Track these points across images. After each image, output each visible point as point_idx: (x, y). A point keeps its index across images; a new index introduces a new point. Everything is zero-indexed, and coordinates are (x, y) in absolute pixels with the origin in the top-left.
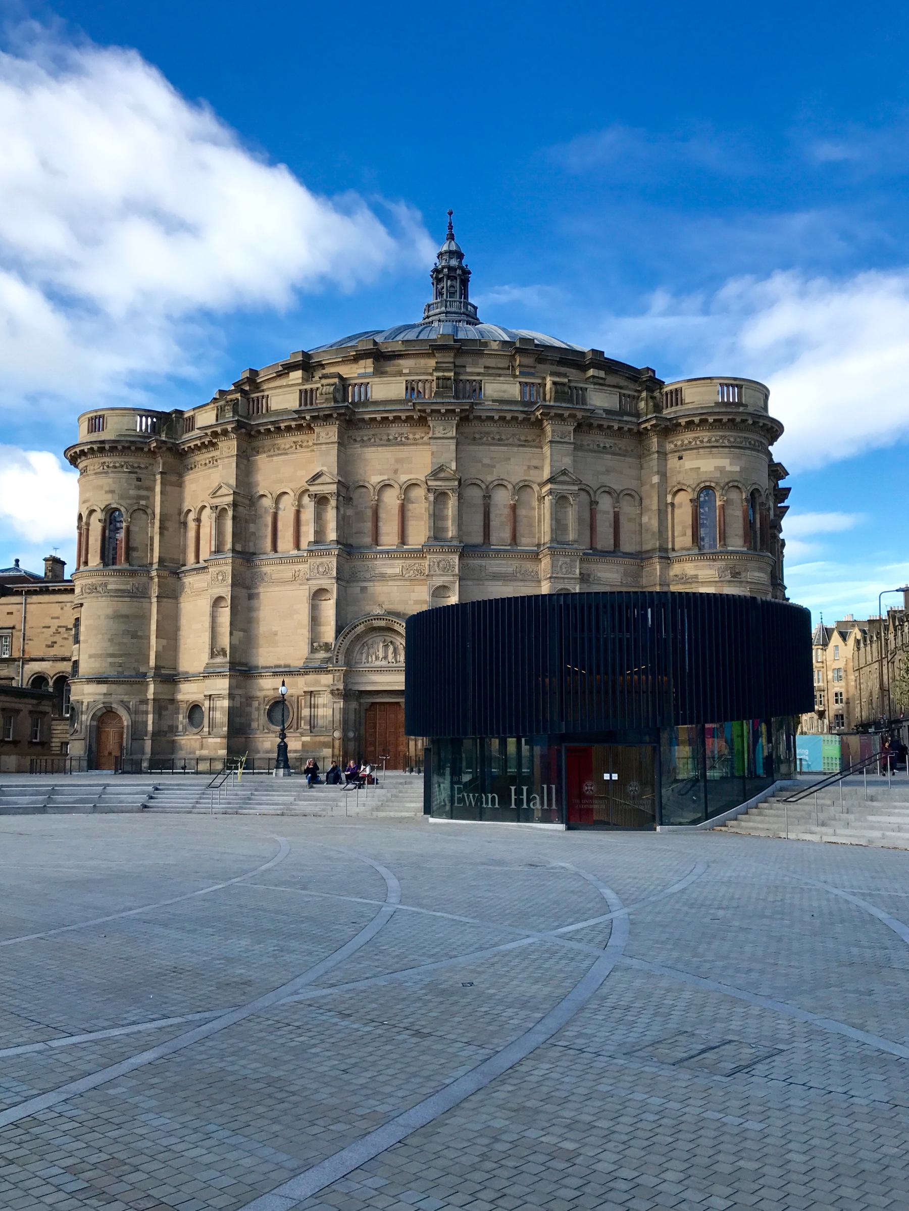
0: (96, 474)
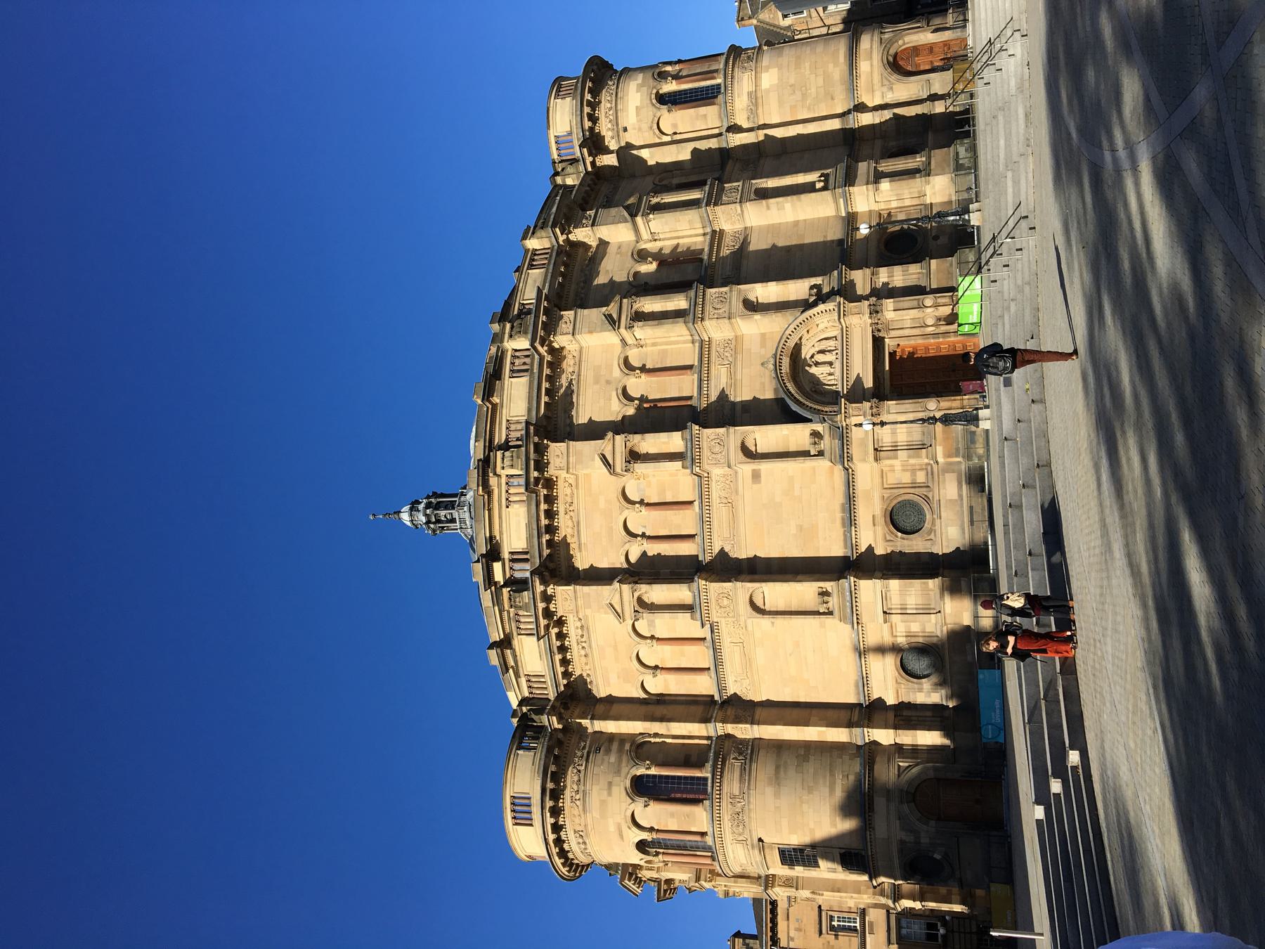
0: (584, 810)
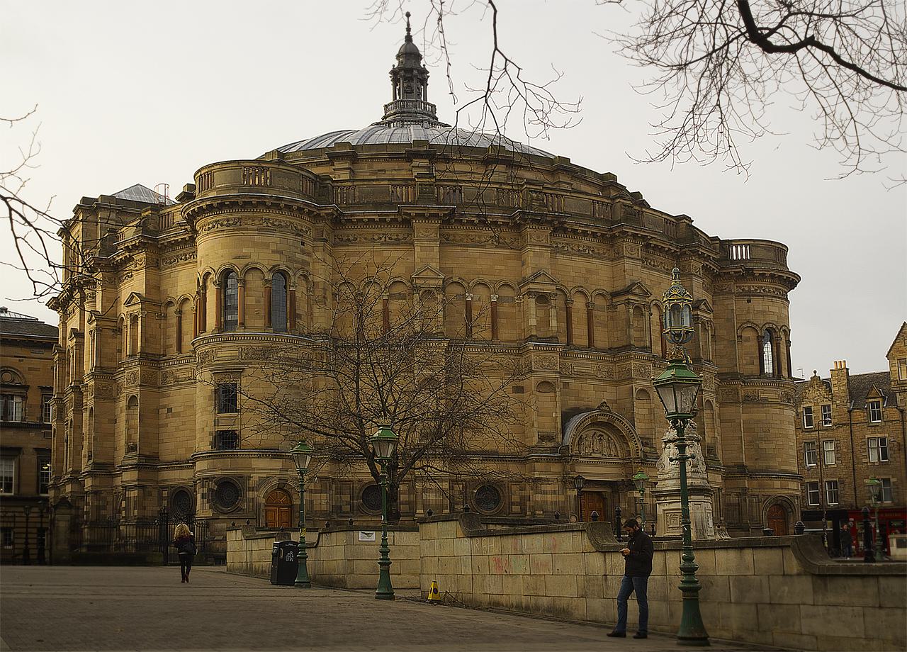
0: (259, 230)
